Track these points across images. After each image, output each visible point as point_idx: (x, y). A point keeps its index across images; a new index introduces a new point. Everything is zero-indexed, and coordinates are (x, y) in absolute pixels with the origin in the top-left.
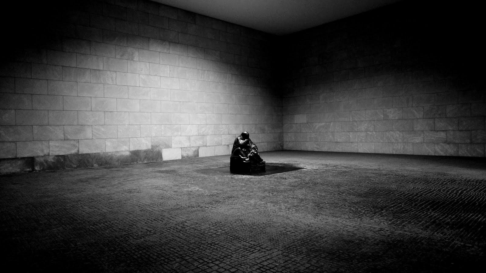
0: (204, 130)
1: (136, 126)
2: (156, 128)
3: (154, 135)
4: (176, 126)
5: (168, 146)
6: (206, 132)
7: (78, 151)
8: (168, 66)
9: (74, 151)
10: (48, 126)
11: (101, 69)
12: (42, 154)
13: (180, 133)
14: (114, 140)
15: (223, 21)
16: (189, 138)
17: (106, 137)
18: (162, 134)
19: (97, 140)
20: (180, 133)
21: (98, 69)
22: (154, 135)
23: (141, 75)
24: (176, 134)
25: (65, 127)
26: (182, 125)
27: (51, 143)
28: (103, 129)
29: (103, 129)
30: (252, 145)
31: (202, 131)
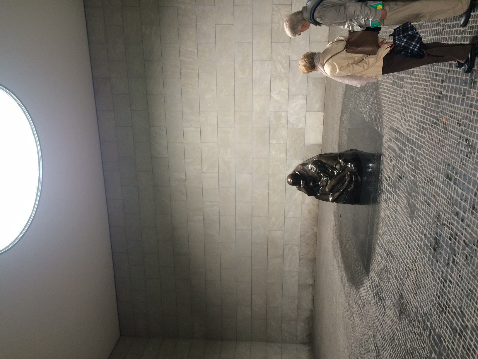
0: (281, 66)
1: (271, 180)
2: (273, 152)
3: (284, 155)
4: (272, 119)
5: (301, 133)
6: (284, 61)
7: (297, 245)
8: (185, 129)
9: (297, 250)
10: (268, 271)
11: (202, 218)
12: (297, 278)
13: (283, 114)
14: (287, 207)
15: (90, 52)
16: (291, 96)
17: (283, 217)
18: (282, 143)
19: (285, 226)
20: (283, 114)
21: (203, 221)
22: (283, 155)
23: (204, 171)
24: (284, 121)
25: (268, 256)
26: (272, 110)
27: (286, 269)
28: (274, 219)
29: (274, 219)
30: (312, 174)
31: (282, 70)
